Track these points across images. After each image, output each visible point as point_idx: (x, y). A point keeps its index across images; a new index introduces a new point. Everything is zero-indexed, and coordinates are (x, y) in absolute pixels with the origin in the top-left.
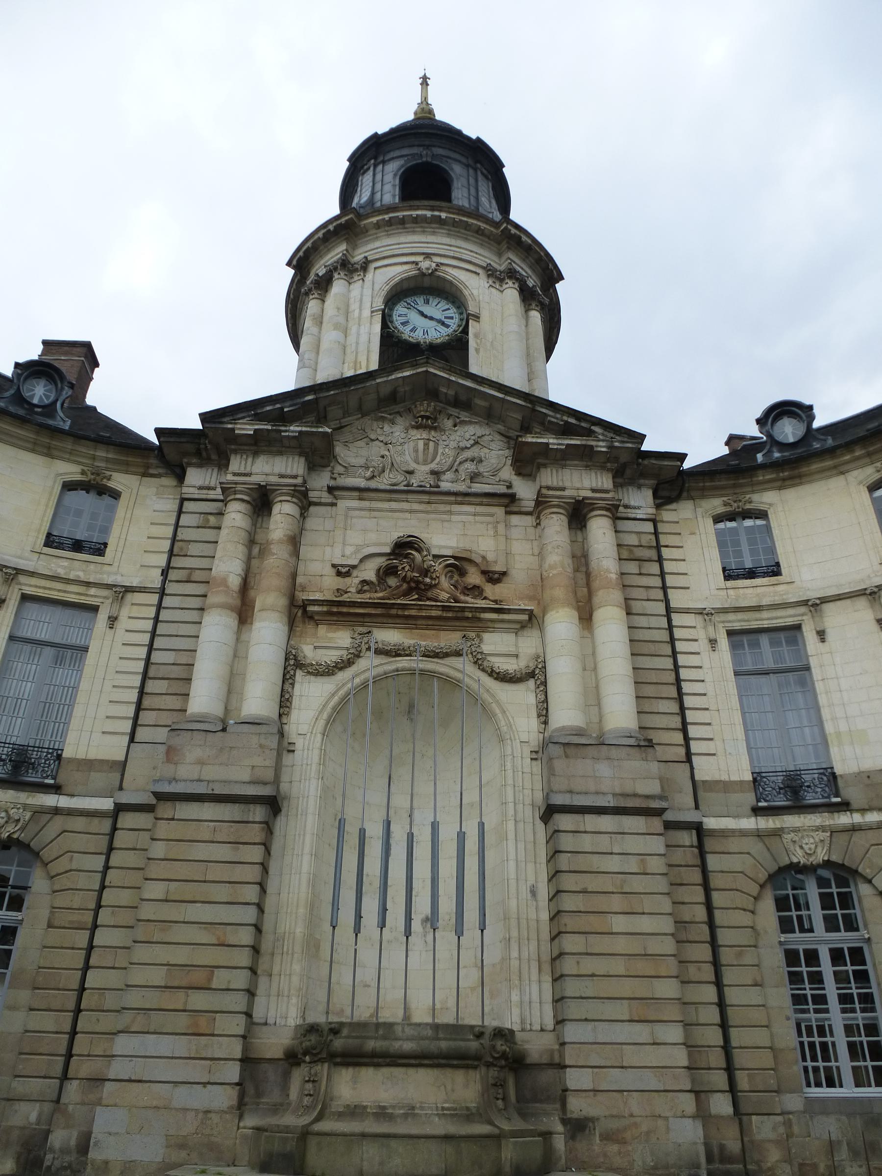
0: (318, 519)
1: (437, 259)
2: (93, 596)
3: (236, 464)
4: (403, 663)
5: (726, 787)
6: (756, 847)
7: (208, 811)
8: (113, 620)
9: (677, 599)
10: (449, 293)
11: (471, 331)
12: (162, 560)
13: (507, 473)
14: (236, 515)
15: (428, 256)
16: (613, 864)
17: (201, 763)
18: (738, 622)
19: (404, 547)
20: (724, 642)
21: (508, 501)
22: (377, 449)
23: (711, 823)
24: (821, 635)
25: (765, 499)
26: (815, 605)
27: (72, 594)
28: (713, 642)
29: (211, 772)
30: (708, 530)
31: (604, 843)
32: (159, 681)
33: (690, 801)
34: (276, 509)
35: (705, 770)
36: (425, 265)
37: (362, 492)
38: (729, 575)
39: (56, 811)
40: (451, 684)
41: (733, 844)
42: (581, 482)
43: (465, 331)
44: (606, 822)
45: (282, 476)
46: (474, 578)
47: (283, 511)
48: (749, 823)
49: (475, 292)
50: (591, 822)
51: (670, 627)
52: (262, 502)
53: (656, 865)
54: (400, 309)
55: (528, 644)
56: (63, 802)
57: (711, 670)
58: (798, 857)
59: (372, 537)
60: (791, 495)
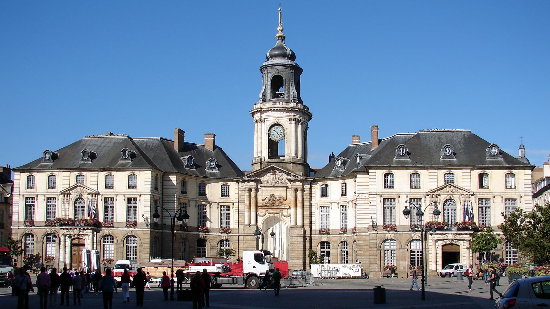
4: (272, 215)
5: (316, 230)
7: (249, 237)
9: (313, 201)
13: (287, 181)
14: (247, 193)
16: (296, 243)
19: (271, 196)
32: (240, 219)
36: (276, 121)
40: (278, 218)
42: (298, 184)
44: (296, 237)
46: (282, 200)
47: (253, 193)
53: (302, 243)
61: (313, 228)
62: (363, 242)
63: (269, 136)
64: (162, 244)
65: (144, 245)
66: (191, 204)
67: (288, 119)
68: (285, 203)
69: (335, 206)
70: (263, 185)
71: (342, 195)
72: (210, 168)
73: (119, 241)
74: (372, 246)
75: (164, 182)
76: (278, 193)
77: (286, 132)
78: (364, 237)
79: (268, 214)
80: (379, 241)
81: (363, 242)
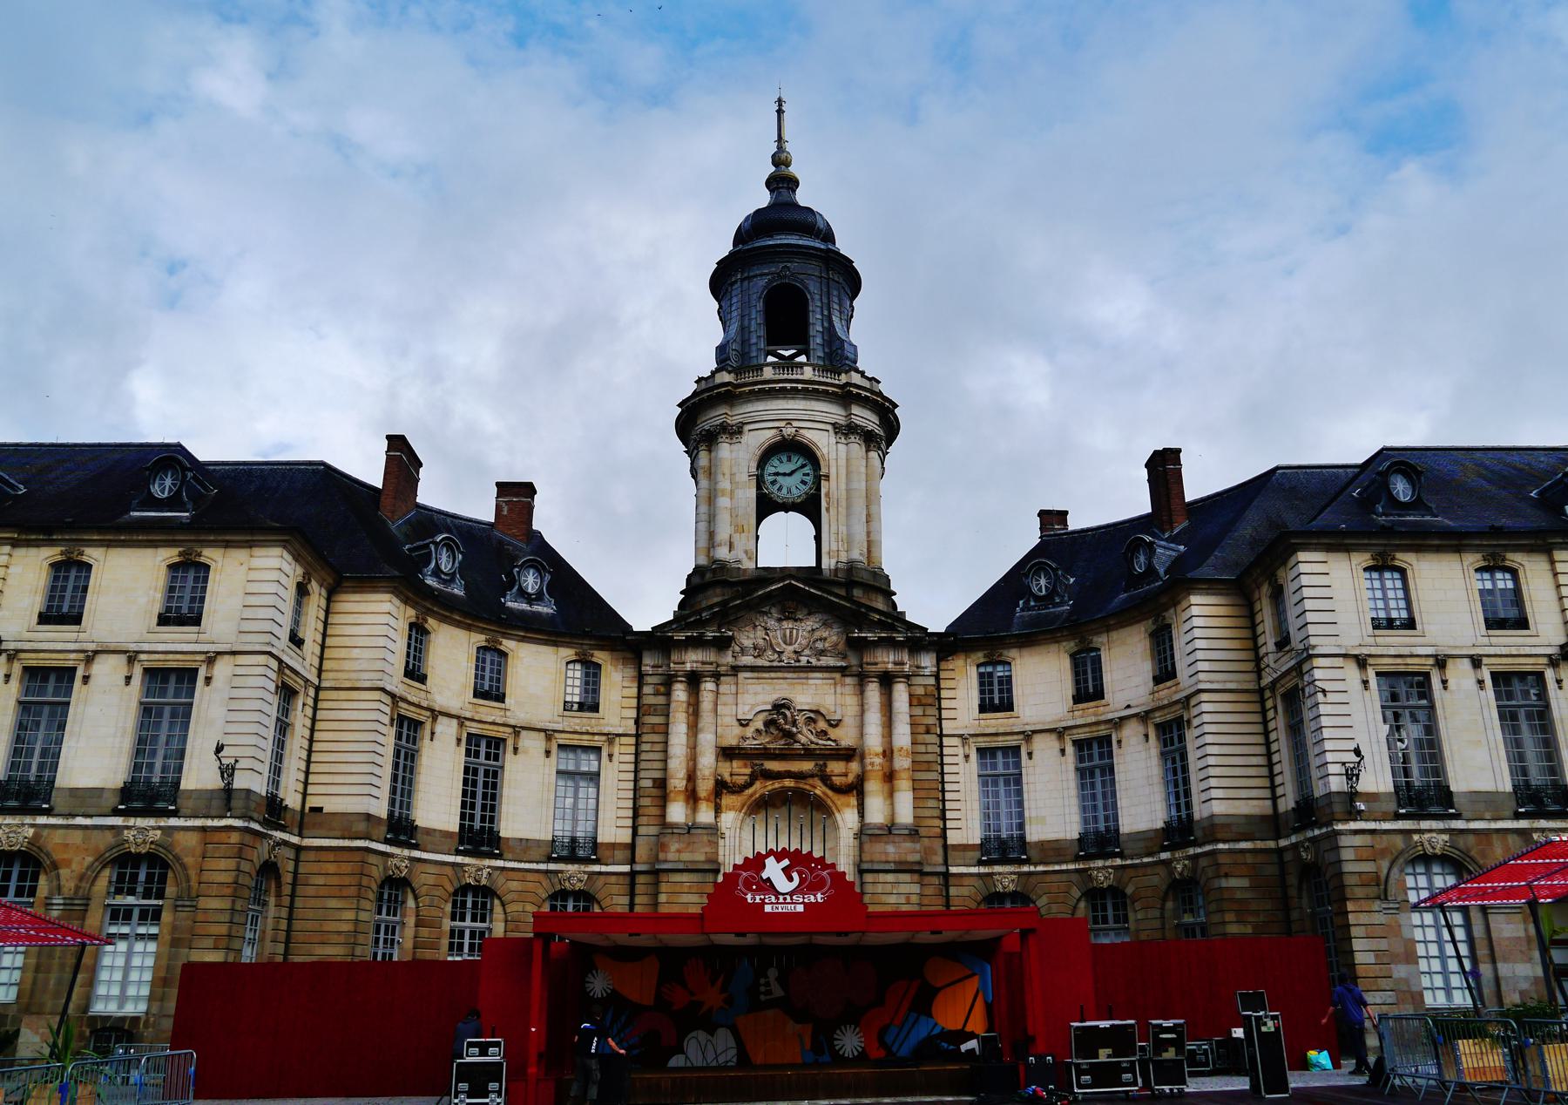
0: (727, 686)
1: (795, 424)
2: (598, 741)
3: (675, 657)
6: (978, 883)
7: (685, 877)
8: (610, 756)
9: (948, 727)
10: (808, 454)
11: (823, 491)
12: (633, 714)
14: (680, 693)
15: (789, 422)
16: (893, 899)
17: (679, 851)
18: (983, 743)
19: (779, 707)
20: (974, 756)
21: (843, 671)
22: (760, 633)
23: (953, 870)
24: (1030, 755)
25: (1012, 653)
26: (1028, 736)
27: (585, 741)
28: (967, 757)
29: (686, 856)
30: (973, 672)
31: (888, 888)
33: (939, 859)
34: (703, 686)
35: (953, 838)
37: (753, 669)
38: (983, 708)
39: (600, 873)
41: (966, 881)
42: (886, 659)
43: (819, 489)
44: (890, 877)
45: (703, 663)
47: (708, 686)
48: (974, 870)
49: (825, 451)
50: (882, 877)
51: (941, 746)
52: (694, 680)
54: (770, 469)
55: (854, 766)
56: (604, 869)
57: (964, 776)
58: (1000, 888)
59: (760, 698)
60: (1025, 652)
61: (953, 838)
62: (1245, 883)
63: (759, 487)
64: (291, 907)
65: (204, 903)
66: (439, 728)
67: (829, 427)
68: (833, 733)
69: (1045, 748)
70: (747, 660)
71: (1078, 699)
72: (523, 594)
73: (69, 885)
74: (1359, 892)
75: (333, 619)
76: (809, 694)
77: (823, 471)
78: (1249, 859)
79: (758, 785)
80: (1385, 864)
81: (1245, 883)
